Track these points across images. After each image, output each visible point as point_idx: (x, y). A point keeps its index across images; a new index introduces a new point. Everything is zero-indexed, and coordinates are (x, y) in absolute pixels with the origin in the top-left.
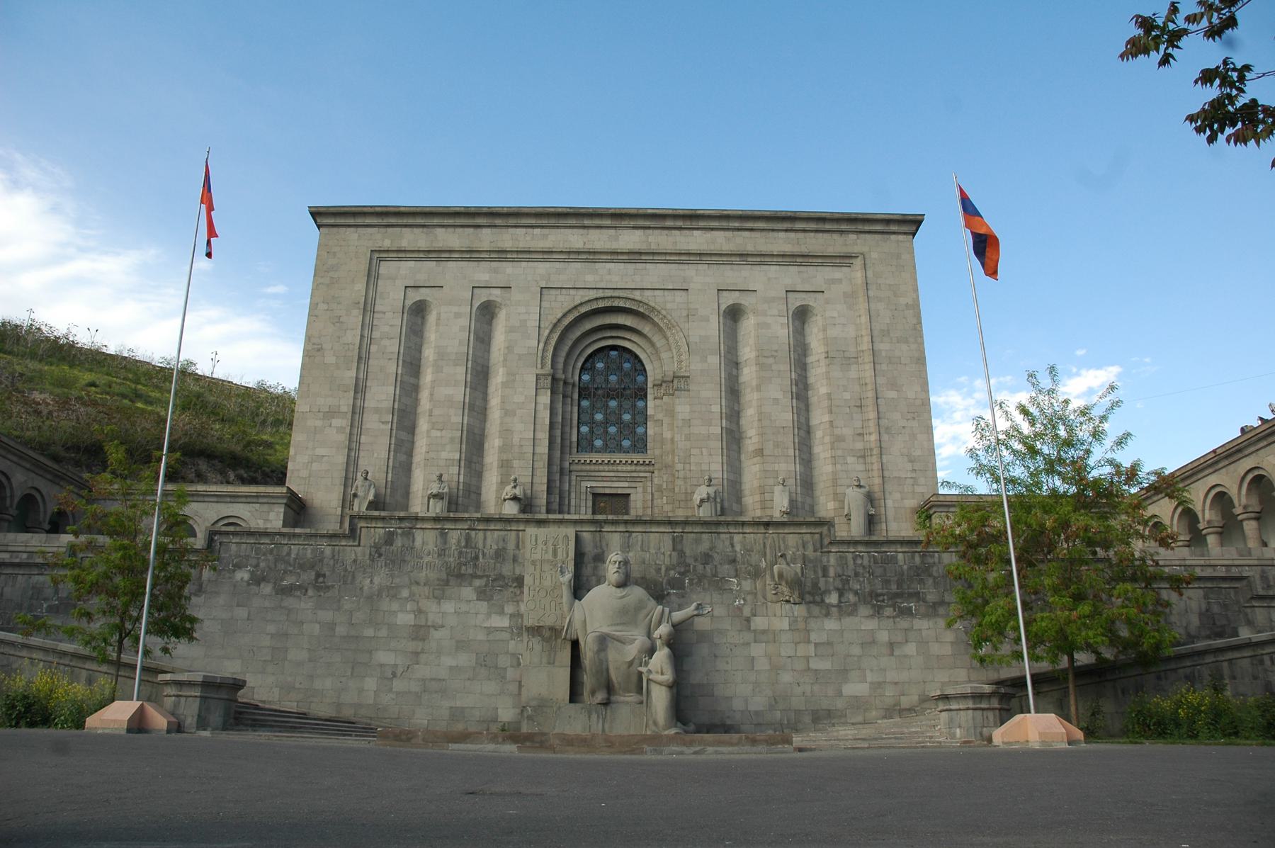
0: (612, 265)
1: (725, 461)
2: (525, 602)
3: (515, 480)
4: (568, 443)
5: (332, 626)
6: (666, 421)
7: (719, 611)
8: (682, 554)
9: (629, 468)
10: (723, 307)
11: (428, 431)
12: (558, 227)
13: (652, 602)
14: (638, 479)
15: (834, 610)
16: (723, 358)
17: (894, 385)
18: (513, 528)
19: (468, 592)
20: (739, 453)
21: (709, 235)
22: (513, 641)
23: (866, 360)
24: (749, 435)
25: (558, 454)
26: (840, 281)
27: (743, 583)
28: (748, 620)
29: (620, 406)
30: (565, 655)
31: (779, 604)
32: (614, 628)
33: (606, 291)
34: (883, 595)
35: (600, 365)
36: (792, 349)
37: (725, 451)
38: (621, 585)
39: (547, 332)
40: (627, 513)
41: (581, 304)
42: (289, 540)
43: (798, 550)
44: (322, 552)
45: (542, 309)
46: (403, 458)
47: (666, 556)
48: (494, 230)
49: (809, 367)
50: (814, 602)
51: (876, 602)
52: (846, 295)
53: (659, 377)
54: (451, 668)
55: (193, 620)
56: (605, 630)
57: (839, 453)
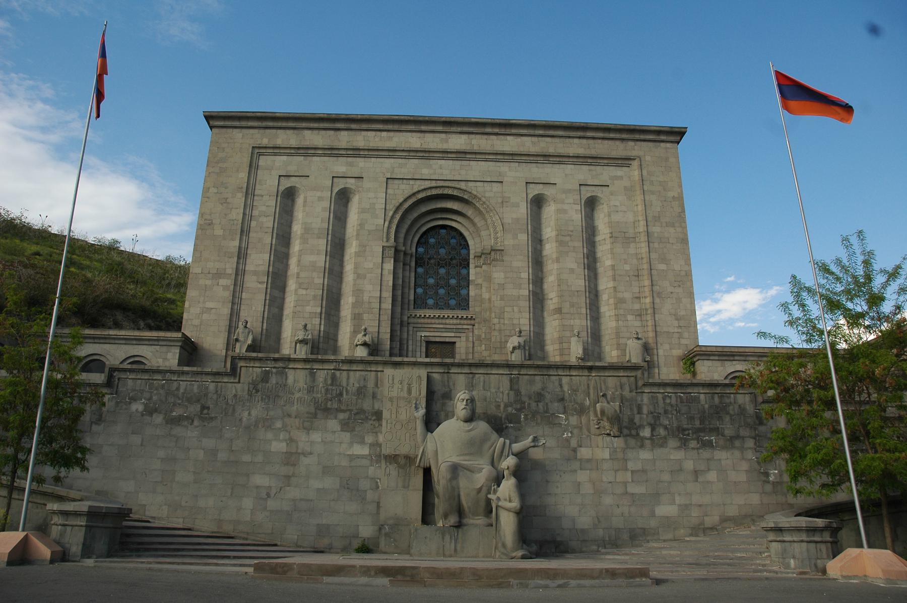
1: (531, 317)
2: (384, 432)
3: (365, 330)
4: (406, 301)
5: (214, 452)
6: (485, 284)
7: (551, 442)
8: (518, 393)
9: (455, 321)
10: (530, 196)
11: (296, 290)
12: (400, 131)
13: (495, 435)
15: (648, 442)
16: (530, 236)
17: (664, 260)
18: (373, 369)
19: (333, 424)
20: (542, 311)
22: (372, 468)
23: (642, 239)
24: (550, 298)
25: (399, 309)
26: (621, 178)
27: (571, 418)
28: (575, 450)
29: (448, 273)
30: (418, 481)
31: (601, 437)
32: (462, 458)
33: (438, 182)
34: (688, 429)
35: (432, 241)
36: (584, 230)
37: (532, 309)
38: (469, 420)
39: (391, 213)
40: (453, 357)
41: (419, 192)
42: (179, 376)
43: (617, 391)
44: (207, 388)
45: (388, 195)
46: (275, 310)
47: (505, 396)
48: (350, 133)
49: (597, 244)
50: (630, 435)
51: (682, 435)
53: (479, 250)
54: (318, 490)
55: (84, 450)
56: (455, 459)
57: (621, 312)
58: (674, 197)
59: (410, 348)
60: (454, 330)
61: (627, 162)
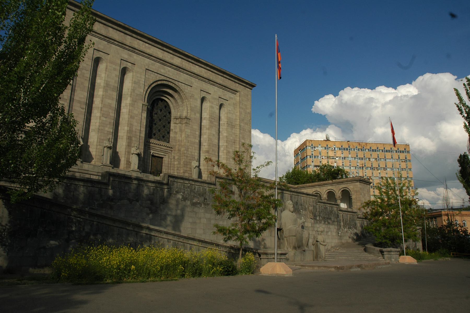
14: (167, 153)
15: (318, 221)
17: (243, 138)
33: (167, 78)
39: (147, 88)
57: (229, 157)
60: (164, 152)
61: (235, 92)
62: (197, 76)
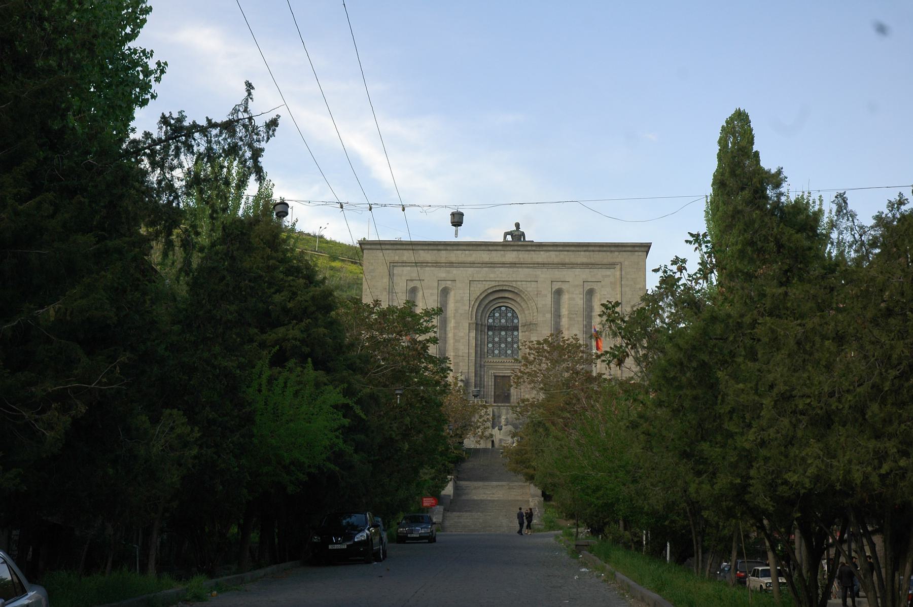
0: (501, 269)
9: (510, 364)
10: (553, 290)
21: (548, 254)
39: (473, 302)
48: (447, 251)
49: (593, 317)
52: (611, 283)
58: (640, 288)
59: (486, 380)
62: (543, 265)
